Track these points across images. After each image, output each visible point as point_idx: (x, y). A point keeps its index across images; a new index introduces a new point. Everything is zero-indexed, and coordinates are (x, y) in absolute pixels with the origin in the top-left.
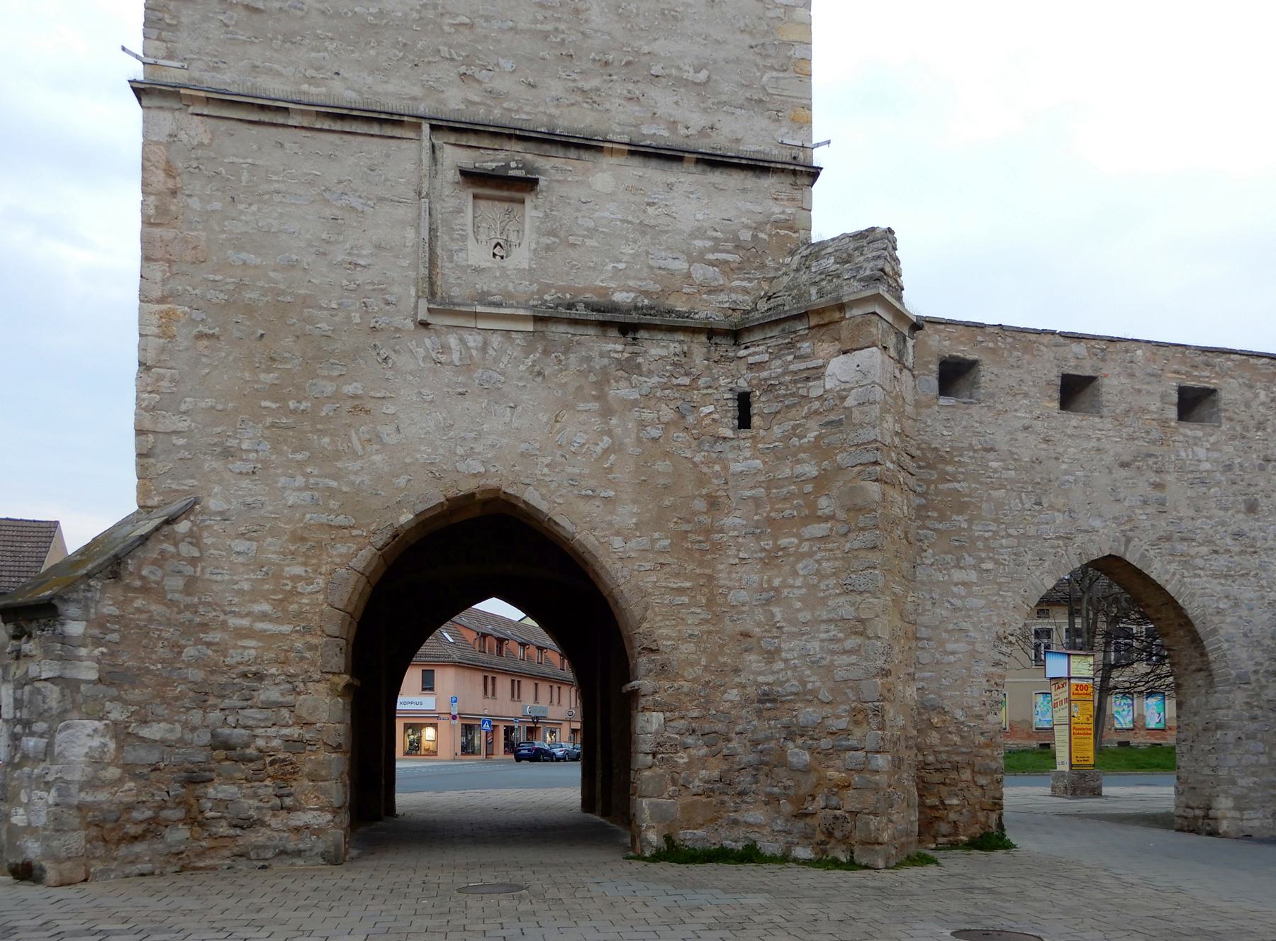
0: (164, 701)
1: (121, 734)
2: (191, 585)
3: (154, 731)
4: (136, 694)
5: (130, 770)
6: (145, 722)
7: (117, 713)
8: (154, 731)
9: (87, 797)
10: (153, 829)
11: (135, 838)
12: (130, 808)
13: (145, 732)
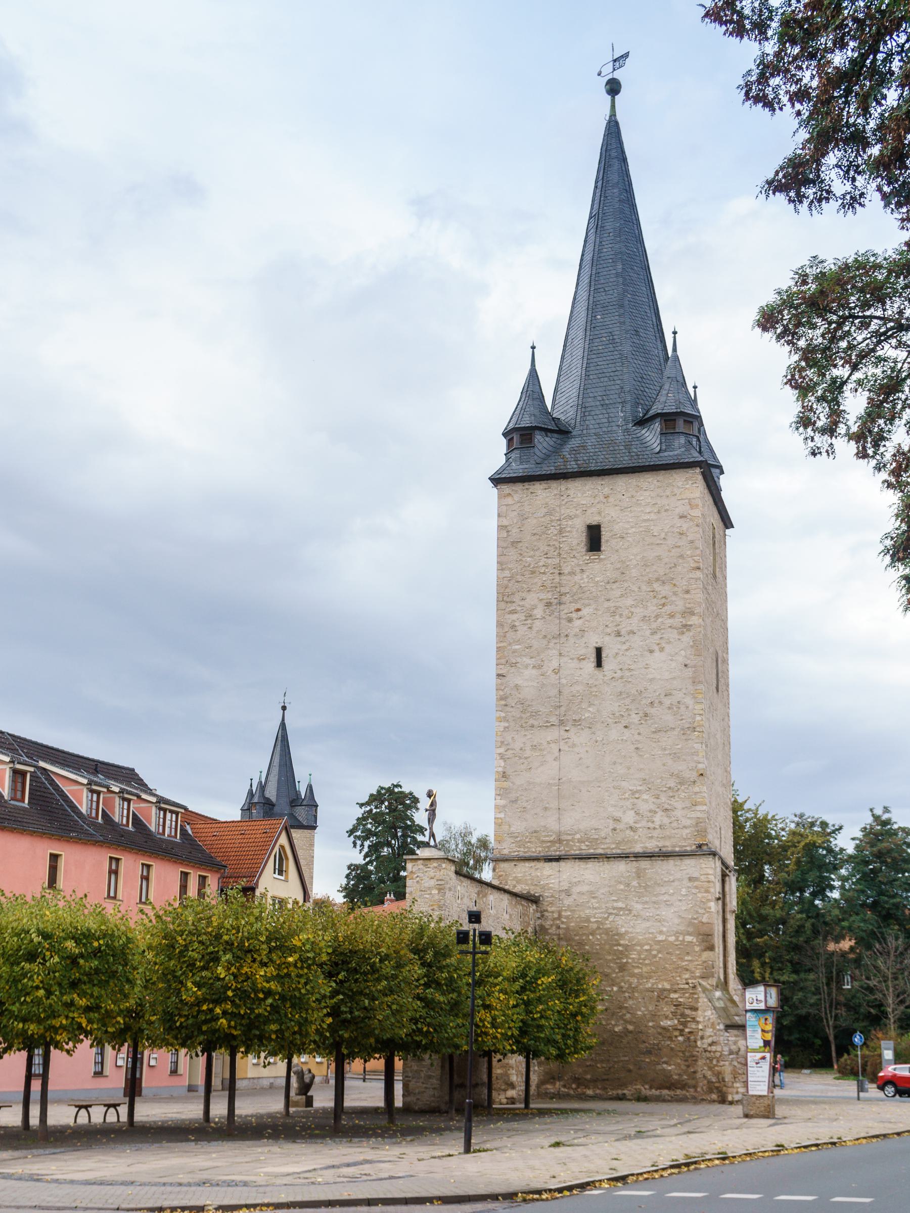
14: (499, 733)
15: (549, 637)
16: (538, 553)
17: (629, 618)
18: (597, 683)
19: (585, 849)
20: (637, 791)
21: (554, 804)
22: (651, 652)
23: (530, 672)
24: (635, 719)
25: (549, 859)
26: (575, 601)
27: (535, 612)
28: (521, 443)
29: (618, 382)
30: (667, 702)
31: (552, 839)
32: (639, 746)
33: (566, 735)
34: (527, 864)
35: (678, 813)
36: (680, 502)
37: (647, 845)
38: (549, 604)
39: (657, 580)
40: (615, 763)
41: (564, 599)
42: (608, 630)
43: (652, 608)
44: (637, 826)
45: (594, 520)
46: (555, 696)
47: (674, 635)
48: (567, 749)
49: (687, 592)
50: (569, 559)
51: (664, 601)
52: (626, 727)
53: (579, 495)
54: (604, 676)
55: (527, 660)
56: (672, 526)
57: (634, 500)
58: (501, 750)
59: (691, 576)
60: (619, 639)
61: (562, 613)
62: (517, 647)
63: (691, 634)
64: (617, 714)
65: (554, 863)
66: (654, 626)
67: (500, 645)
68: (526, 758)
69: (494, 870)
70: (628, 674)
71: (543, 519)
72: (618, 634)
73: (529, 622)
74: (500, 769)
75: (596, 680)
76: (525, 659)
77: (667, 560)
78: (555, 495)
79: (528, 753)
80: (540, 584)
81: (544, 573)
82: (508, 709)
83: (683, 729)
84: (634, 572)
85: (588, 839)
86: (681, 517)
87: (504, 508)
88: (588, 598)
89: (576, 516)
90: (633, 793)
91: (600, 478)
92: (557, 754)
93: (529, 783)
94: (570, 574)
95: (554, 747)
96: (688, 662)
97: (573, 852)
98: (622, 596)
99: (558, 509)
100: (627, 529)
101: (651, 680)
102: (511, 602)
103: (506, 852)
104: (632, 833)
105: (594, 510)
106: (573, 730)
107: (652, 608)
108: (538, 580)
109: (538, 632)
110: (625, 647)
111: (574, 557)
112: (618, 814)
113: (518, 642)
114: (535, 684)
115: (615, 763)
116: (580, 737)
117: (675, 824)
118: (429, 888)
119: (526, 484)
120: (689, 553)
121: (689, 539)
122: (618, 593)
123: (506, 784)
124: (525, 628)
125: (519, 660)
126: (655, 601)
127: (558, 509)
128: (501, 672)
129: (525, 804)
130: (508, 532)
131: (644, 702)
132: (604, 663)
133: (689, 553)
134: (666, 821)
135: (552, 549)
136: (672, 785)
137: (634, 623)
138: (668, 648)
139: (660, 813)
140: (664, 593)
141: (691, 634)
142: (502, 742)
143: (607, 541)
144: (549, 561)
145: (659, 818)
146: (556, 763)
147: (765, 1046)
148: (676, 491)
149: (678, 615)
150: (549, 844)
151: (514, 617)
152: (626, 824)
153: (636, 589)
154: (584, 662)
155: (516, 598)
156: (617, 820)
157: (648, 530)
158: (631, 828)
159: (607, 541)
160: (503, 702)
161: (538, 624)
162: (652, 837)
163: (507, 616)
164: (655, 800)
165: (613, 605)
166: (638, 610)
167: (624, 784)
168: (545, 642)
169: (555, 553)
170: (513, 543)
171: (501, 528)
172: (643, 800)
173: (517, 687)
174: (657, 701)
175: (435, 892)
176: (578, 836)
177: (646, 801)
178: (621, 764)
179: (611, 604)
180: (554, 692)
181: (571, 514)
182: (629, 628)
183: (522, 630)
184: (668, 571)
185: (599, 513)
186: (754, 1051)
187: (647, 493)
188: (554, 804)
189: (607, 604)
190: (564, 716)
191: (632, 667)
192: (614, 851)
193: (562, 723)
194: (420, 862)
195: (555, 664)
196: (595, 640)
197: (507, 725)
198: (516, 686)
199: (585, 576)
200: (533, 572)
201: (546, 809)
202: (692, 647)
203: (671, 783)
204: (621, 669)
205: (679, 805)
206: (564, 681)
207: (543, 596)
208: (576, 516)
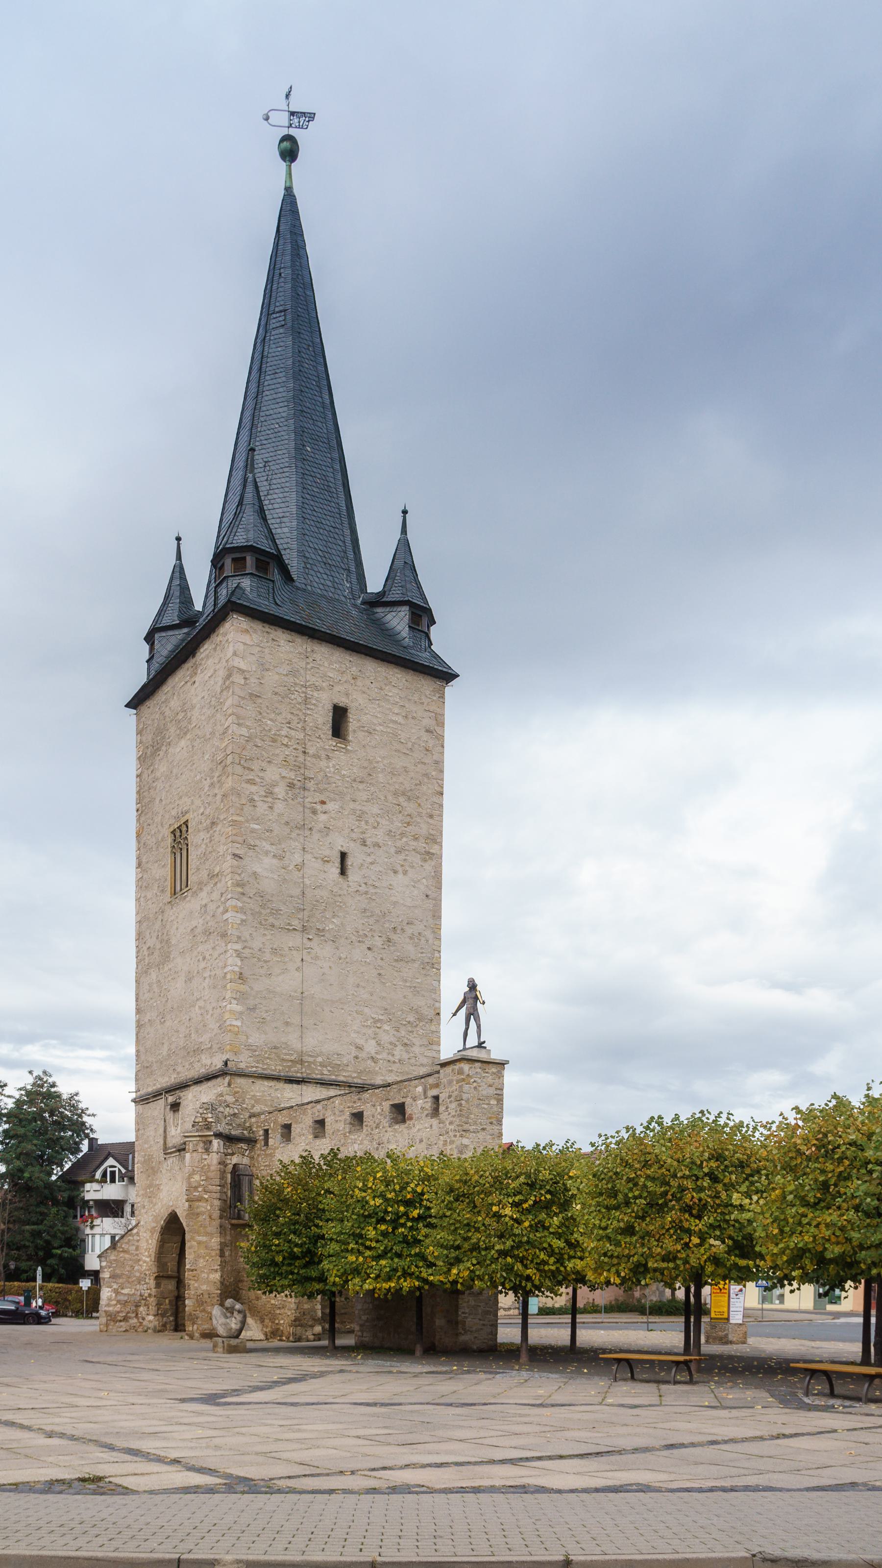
1: (117, 1292)
3: (126, 1291)
4: (121, 1281)
5: (119, 1302)
6: (122, 1289)
7: (115, 1286)
8: (126, 1291)
9: (107, 1309)
10: (125, 1319)
11: (120, 1321)
12: (118, 1312)
13: (123, 1291)
14: (235, 926)
15: (292, 824)
17: (375, 828)
18: (341, 892)
19: (327, 1074)
20: (379, 1020)
22: (395, 872)
23: (268, 861)
24: (378, 942)
25: (290, 1081)
26: (321, 791)
27: (276, 790)
30: (409, 930)
31: (293, 1058)
32: (381, 972)
33: (308, 944)
34: (266, 1083)
35: (417, 1050)
36: (428, 713)
37: (387, 1078)
38: (291, 786)
41: (310, 785)
42: (354, 836)
44: (379, 1057)
45: (342, 701)
46: (298, 897)
47: (416, 859)
48: (309, 960)
49: (431, 816)
50: (313, 738)
52: (369, 949)
54: (349, 886)
55: (268, 847)
61: (307, 800)
63: (433, 863)
64: (361, 933)
65: (295, 1086)
66: (399, 844)
68: (266, 962)
69: (229, 1085)
70: (372, 890)
72: (364, 843)
75: (341, 889)
76: (264, 844)
77: (412, 774)
79: (267, 956)
82: (245, 899)
83: (423, 963)
85: (330, 1064)
86: (428, 731)
88: (333, 792)
90: (376, 1021)
92: (299, 964)
94: (314, 756)
95: (297, 956)
97: (314, 1076)
98: (368, 801)
100: (375, 725)
101: (395, 903)
102: (248, 769)
103: (242, 1065)
104: (373, 1064)
106: (316, 940)
107: (397, 825)
109: (279, 815)
110: (369, 860)
111: (319, 737)
112: (361, 1042)
114: (276, 877)
116: (325, 951)
117: (413, 1061)
122: (363, 796)
123: (242, 988)
124: (266, 806)
125: (258, 842)
126: (400, 816)
131: (387, 925)
132: (350, 872)
134: (405, 1056)
136: (412, 1019)
137: (379, 836)
139: (400, 1047)
140: (409, 810)
143: (354, 731)
144: (293, 733)
145: (399, 1052)
146: (297, 974)
148: (424, 700)
149: (422, 840)
150: (289, 1064)
152: (368, 1053)
153: (383, 798)
154: (329, 865)
155: (255, 766)
156: (359, 1048)
158: (372, 1058)
159: (354, 731)
160: (240, 890)
161: (279, 806)
162: (391, 1071)
164: (396, 1033)
165: (359, 807)
166: (383, 822)
167: (366, 1010)
169: (300, 726)
172: (384, 1031)
174: (400, 927)
176: (320, 1059)
178: (364, 987)
180: (297, 892)
184: (413, 787)
185: (347, 695)
187: (395, 691)
188: (296, 1020)
189: (352, 805)
192: (356, 1081)
193: (304, 929)
195: (298, 858)
196: (341, 843)
197: (244, 918)
198: (255, 873)
199: (331, 765)
201: (287, 1024)
202: (433, 877)
203: (411, 1018)
204: (366, 884)
205: (417, 1042)
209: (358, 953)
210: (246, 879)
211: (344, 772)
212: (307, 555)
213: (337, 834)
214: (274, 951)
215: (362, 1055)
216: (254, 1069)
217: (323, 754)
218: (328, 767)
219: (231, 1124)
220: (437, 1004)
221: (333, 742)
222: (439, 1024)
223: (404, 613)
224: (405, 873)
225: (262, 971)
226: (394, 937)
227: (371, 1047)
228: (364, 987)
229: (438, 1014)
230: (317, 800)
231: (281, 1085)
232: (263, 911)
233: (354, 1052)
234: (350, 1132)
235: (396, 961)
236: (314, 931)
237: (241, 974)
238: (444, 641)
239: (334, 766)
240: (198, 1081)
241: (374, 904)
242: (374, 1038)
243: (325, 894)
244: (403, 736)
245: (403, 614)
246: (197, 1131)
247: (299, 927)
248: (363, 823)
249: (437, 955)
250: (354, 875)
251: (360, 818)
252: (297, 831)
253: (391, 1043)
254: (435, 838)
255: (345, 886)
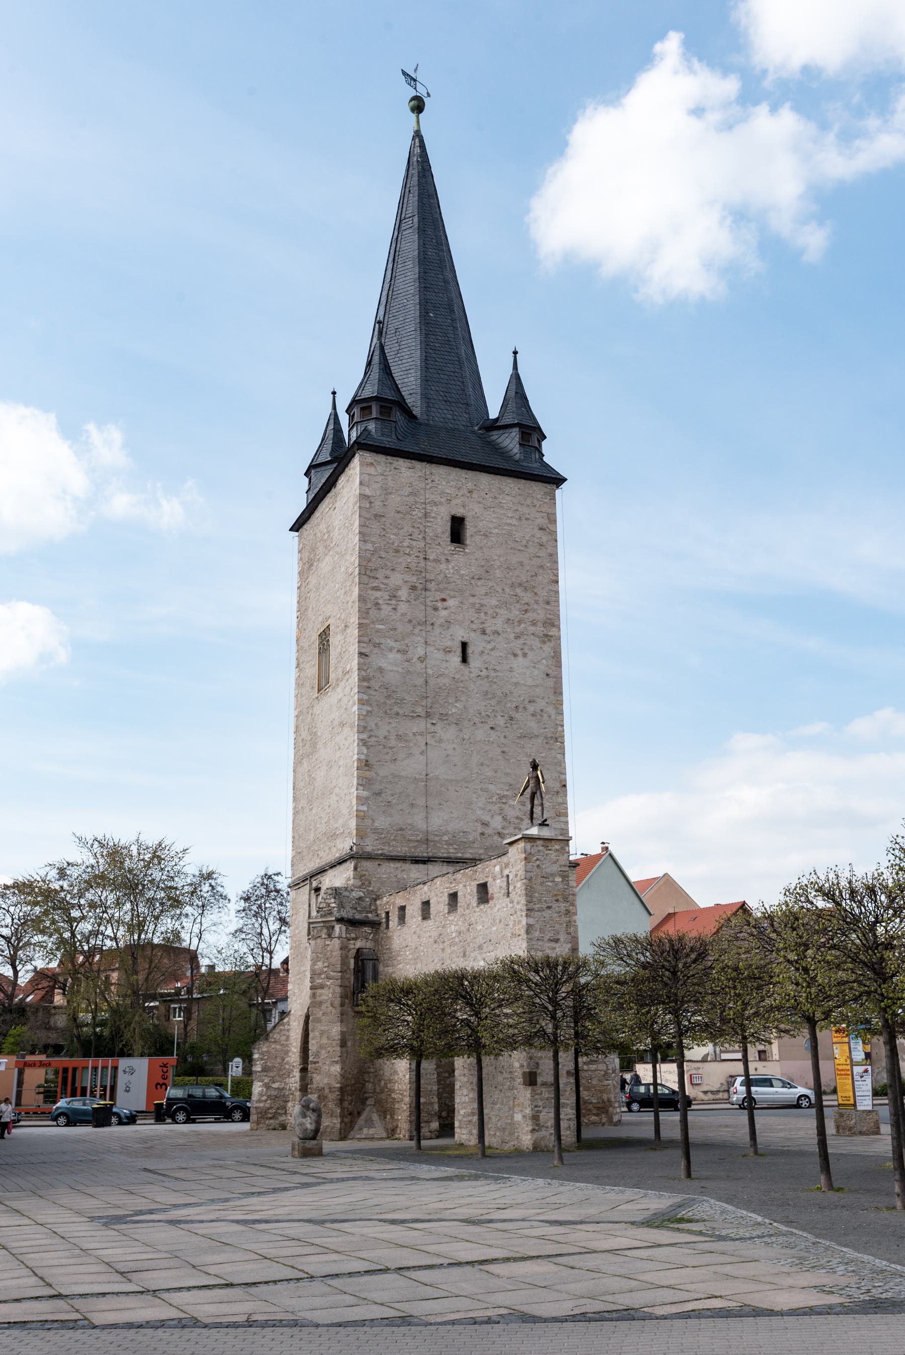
0: (279, 1076)
1: (268, 1086)
2: (288, 1038)
3: (275, 1085)
4: (272, 1074)
8: (275, 1085)
9: (258, 1105)
11: (271, 1118)
12: (269, 1109)
14: (361, 717)
15: (414, 622)
16: (402, 532)
17: (494, 617)
19: (452, 852)
20: (504, 796)
21: (421, 801)
22: (515, 655)
23: (393, 656)
24: (501, 721)
25: (417, 861)
26: (441, 590)
27: (399, 593)
28: (381, 413)
29: (459, 383)
30: (531, 708)
31: (419, 838)
32: (505, 749)
33: (432, 728)
34: (392, 865)
36: (540, 514)
38: (414, 588)
39: (520, 585)
40: (482, 764)
41: (429, 586)
42: (474, 626)
43: (515, 613)
44: (505, 832)
45: (459, 512)
46: (421, 686)
47: (536, 643)
48: (434, 744)
49: (548, 603)
50: (434, 545)
51: (526, 607)
52: (492, 728)
53: (444, 483)
54: (470, 672)
55: (391, 643)
56: (533, 536)
57: (497, 501)
58: (364, 736)
59: (551, 588)
60: (484, 637)
62: (381, 627)
63: (552, 645)
64: (483, 714)
65: (421, 866)
66: (517, 630)
67: (362, 621)
68: (391, 748)
69: (355, 868)
70: (493, 674)
71: (407, 499)
72: (484, 632)
73: (393, 602)
74: (363, 757)
76: (389, 641)
77: (528, 568)
78: (420, 477)
79: (393, 743)
80: (404, 565)
81: (409, 554)
82: (371, 692)
83: (546, 738)
84: (498, 573)
86: (541, 529)
87: (366, 477)
89: (441, 504)
90: (501, 797)
91: (464, 471)
93: (395, 776)
95: (421, 741)
96: (550, 672)
97: (441, 855)
98: (486, 594)
99: (422, 492)
100: (490, 528)
101: (516, 684)
103: (369, 849)
104: (500, 839)
105: (458, 501)
107: (515, 613)
108: (403, 561)
109: (402, 615)
110: (489, 647)
112: (487, 818)
113: (381, 621)
114: (400, 670)
115: (482, 764)
116: (449, 733)
118: (552, 875)
119: (388, 457)
120: (548, 565)
121: (548, 551)
123: (368, 774)
125: (382, 641)
126: (518, 606)
127: (422, 492)
128: (363, 651)
129: (390, 799)
130: (371, 503)
131: (509, 705)
133: (548, 565)
135: (417, 531)
137: (499, 624)
138: (531, 655)
140: (526, 600)
141: (552, 645)
142: (365, 727)
143: (472, 536)
144: (414, 543)
146: (422, 758)
147: (866, 1059)
148: (538, 503)
151: (378, 594)
152: (494, 829)
153: (500, 591)
154: (451, 655)
156: (485, 824)
157: (510, 534)
158: (499, 833)
161: (403, 607)
163: (370, 592)
164: (521, 807)
165: (478, 601)
166: (502, 612)
167: (491, 787)
168: (409, 627)
169: (420, 537)
170: (376, 516)
171: (363, 497)
172: (510, 806)
173: (381, 670)
174: (521, 706)
175: (558, 879)
176: (446, 838)
177: (513, 807)
178: (488, 766)
179: (475, 600)
180: (420, 681)
181: (436, 500)
182: (494, 628)
183: (386, 610)
184: (529, 579)
186: (859, 1064)
187: (509, 498)
188: (421, 801)
189: (472, 600)
190: (431, 706)
191: (497, 668)
193: (428, 715)
194: (539, 842)
195: (420, 651)
196: (460, 634)
197: (370, 709)
199: (450, 567)
200: (397, 551)
201: (412, 805)
202: (553, 657)
204: (487, 668)
206: (430, 671)
207: (408, 577)
208: (441, 504)
209: (481, 733)
210: (371, 674)
211: (462, 572)
212: (430, 396)
213: (457, 626)
214: (399, 737)
215: (488, 831)
216: (380, 852)
217: (443, 559)
218: (447, 569)
219: (356, 909)
220: (562, 776)
221: (452, 547)
222: (566, 796)
223: (515, 433)
224: (525, 655)
225: (388, 757)
226: (517, 716)
227: (497, 823)
228: (488, 766)
229: (565, 786)
230: (438, 598)
231: (407, 866)
232: (388, 702)
233: (480, 829)
234: (449, 912)
235: (519, 738)
236: (437, 716)
237: (367, 761)
238: (553, 454)
239: (453, 568)
240: (332, 866)
241: (495, 687)
242: (500, 814)
243: (446, 681)
244: (518, 536)
245: (514, 434)
246: (322, 916)
247: (423, 714)
248: (482, 614)
249: (560, 729)
250: (475, 661)
251: (478, 611)
252: (420, 628)
253: (517, 818)
254: (553, 622)
255: (467, 673)
